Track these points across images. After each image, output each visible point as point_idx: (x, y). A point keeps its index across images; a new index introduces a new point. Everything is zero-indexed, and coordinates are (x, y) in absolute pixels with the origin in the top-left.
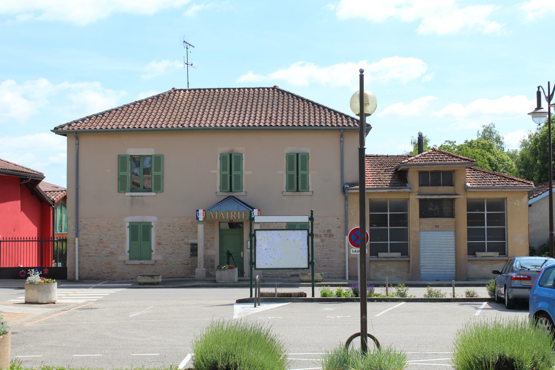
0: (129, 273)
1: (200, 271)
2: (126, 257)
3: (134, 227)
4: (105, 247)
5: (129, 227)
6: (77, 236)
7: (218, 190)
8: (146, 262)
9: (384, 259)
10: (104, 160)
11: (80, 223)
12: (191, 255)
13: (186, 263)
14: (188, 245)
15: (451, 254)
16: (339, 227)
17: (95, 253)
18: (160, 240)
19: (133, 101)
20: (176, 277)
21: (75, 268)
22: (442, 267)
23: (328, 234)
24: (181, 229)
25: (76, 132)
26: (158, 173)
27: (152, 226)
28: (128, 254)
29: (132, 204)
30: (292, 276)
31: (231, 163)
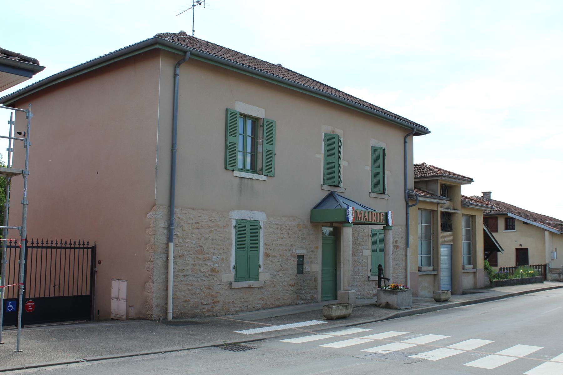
2: (229, 276)
3: (241, 227)
4: (205, 260)
5: (235, 227)
13: (292, 282)
17: (193, 270)
24: (288, 233)
27: (260, 228)
28: (233, 271)
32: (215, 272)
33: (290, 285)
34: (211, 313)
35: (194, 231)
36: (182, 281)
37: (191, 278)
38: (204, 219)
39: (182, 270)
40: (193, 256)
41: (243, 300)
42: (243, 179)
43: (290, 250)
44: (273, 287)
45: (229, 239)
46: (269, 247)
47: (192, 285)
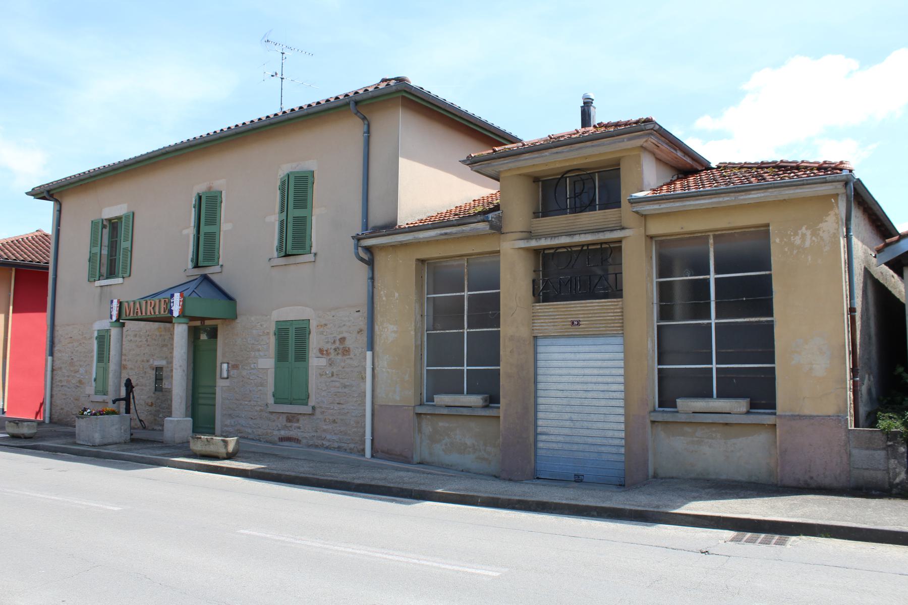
13: (150, 401)
15: (614, 403)
22: (590, 440)
30: (282, 439)
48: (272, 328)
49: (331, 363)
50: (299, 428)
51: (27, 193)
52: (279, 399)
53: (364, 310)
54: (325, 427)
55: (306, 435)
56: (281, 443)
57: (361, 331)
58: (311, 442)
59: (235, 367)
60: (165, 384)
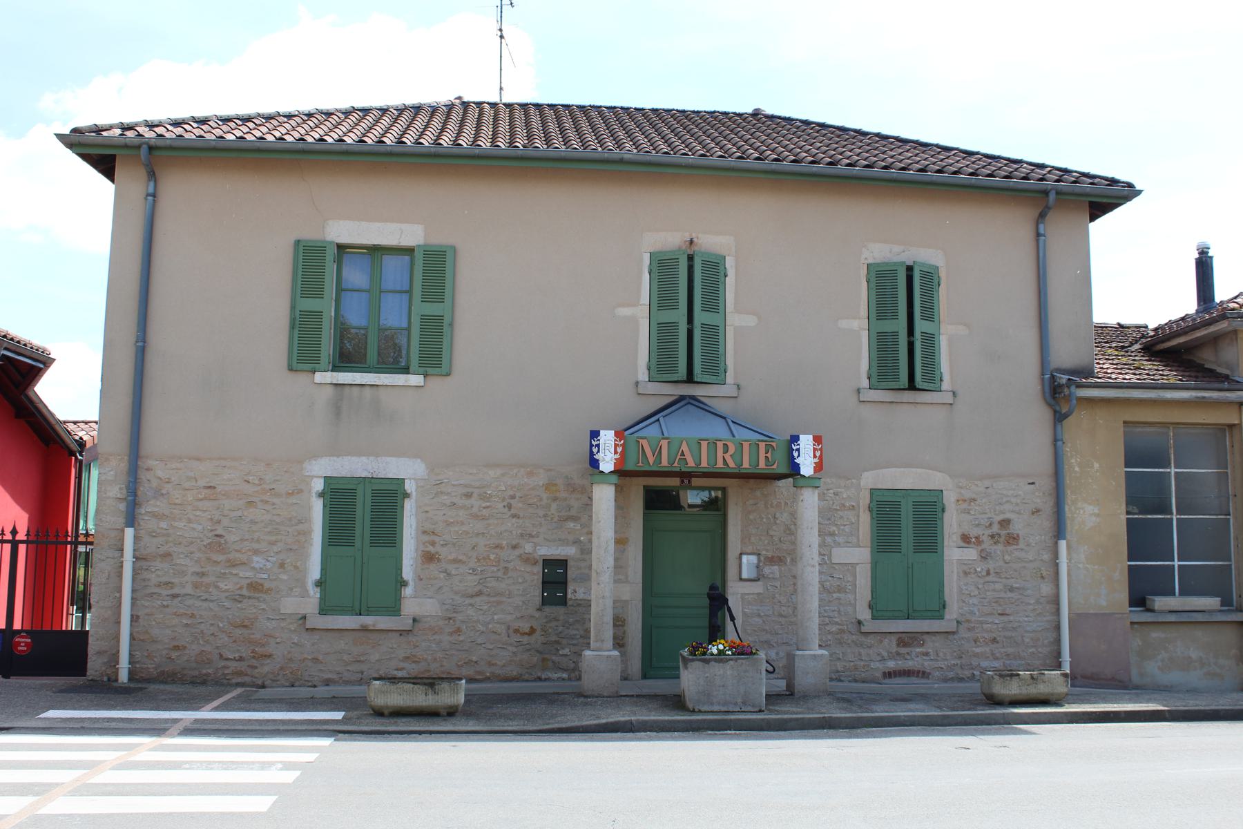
0: (315, 660)
1: (600, 659)
2: (310, 601)
3: (339, 495)
4: (233, 564)
5: (321, 494)
6: (131, 520)
7: (643, 375)
8: (383, 622)
9: (1173, 618)
10: (242, 252)
11: (143, 476)
12: (545, 602)
14: (536, 563)
16: (1036, 512)
17: (196, 586)
18: (433, 544)
19: (345, 105)
20: (487, 679)
21: (117, 638)
23: (1003, 533)
24: (510, 507)
25: (151, 148)
26: (432, 309)
27: (407, 495)
28: (314, 593)
29: (337, 409)
30: (889, 675)
31: (688, 289)
32: (261, 591)
33: (517, 631)
34: (247, 679)
35: (200, 504)
36: (164, 606)
37: (190, 602)
38: (230, 480)
39: (166, 584)
40: (197, 555)
41: (345, 657)
42: (347, 389)
43: (514, 547)
44: (451, 634)
45: (306, 520)
46: (436, 539)
47: (193, 616)
48: (865, 500)
49: (984, 556)
50: (927, 654)
51: (57, 135)
52: (877, 610)
53: (1046, 483)
54: (978, 650)
55: (942, 664)
56: (887, 681)
57: (1038, 511)
58: (951, 675)
59: (771, 561)
60: (575, 591)
